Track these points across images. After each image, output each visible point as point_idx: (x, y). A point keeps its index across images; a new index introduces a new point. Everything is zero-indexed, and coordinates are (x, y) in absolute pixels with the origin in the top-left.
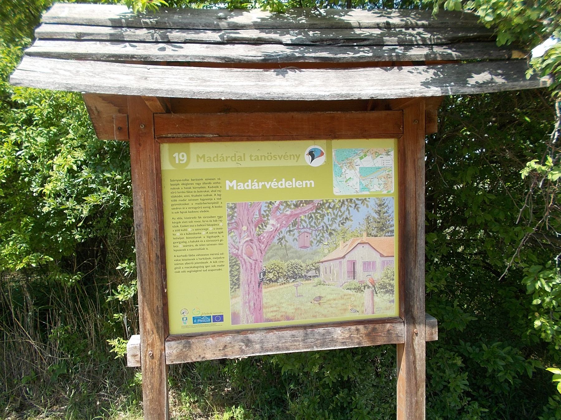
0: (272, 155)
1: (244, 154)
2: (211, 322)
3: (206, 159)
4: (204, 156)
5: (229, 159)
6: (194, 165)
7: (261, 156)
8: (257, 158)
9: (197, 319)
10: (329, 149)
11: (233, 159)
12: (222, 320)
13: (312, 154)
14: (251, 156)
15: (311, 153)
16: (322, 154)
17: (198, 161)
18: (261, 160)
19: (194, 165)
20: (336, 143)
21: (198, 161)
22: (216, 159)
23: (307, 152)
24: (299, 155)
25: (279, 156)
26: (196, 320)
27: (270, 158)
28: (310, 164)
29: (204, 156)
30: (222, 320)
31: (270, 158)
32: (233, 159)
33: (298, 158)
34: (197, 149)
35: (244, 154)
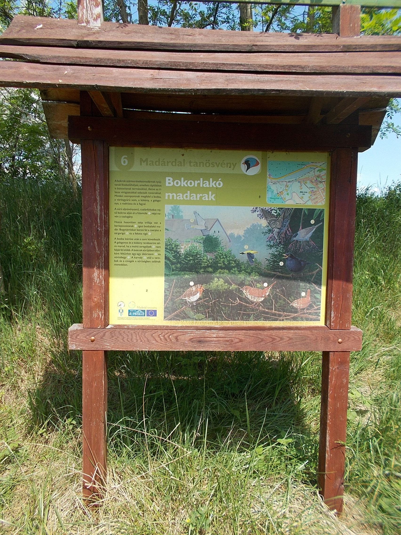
1: (184, 160)
2: (144, 315)
5: (170, 164)
11: (174, 164)
12: (155, 315)
13: (248, 164)
16: (257, 164)
17: (141, 164)
18: (200, 166)
22: (157, 163)
23: (243, 161)
24: (236, 164)
25: (216, 163)
26: (131, 313)
28: (245, 173)
30: (155, 315)
31: (208, 164)
32: (174, 164)
35: (184, 160)
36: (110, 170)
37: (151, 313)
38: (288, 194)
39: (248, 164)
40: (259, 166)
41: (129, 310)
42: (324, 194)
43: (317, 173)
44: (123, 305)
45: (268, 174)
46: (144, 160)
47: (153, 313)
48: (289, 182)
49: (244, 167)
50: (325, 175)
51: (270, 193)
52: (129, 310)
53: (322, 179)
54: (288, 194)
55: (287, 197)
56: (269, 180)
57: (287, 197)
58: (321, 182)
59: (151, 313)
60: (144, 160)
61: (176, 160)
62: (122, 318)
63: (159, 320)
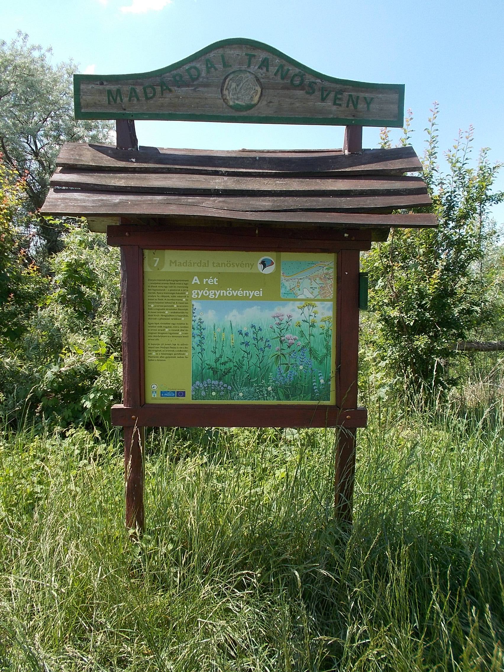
0: (231, 263)
2: (175, 396)
3: (177, 264)
4: (175, 261)
6: (167, 268)
7: (222, 264)
8: (218, 265)
9: (164, 393)
10: (278, 260)
12: (184, 396)
13: (264, 264)
14: (213, 263)
15: (263, 263)
16: (273, 263)
17: (171, 265)
19: (167, 268)
20: (285, 256)
21: (171, 265)
22: (185, 264)
23: (260, 261)
26: (163, 394)
27: (229, 265)
29: (175, 261)
30: (184, 396)
31: (229, 265)
32: (199, 264)
33: (252, 266)
34: (171, 255)
36: (145, 270)
37: (181, 394)
38: (299, 290)
39: (264, 264)
40: (273, 266)
41: (161, 392)
42: (332, 289)
43: (325, 271)
44: (155, 388)
45: (282, 272)
46: (173, 261)
47: (182, 394)
48: (301, 279)
49: (261, 267)
50: (332, 272)
51: (283, 289)
52: (161, 392)
53: (330, 276)
54: (299, 290)
55: (299, 292)
56: (282, 277)
57: (299, 292)
58: (329, 279)
59: (181, 394)
60: (173, 261)
61: (201, 261)
62: (155, 399)
63: (188, 400)
